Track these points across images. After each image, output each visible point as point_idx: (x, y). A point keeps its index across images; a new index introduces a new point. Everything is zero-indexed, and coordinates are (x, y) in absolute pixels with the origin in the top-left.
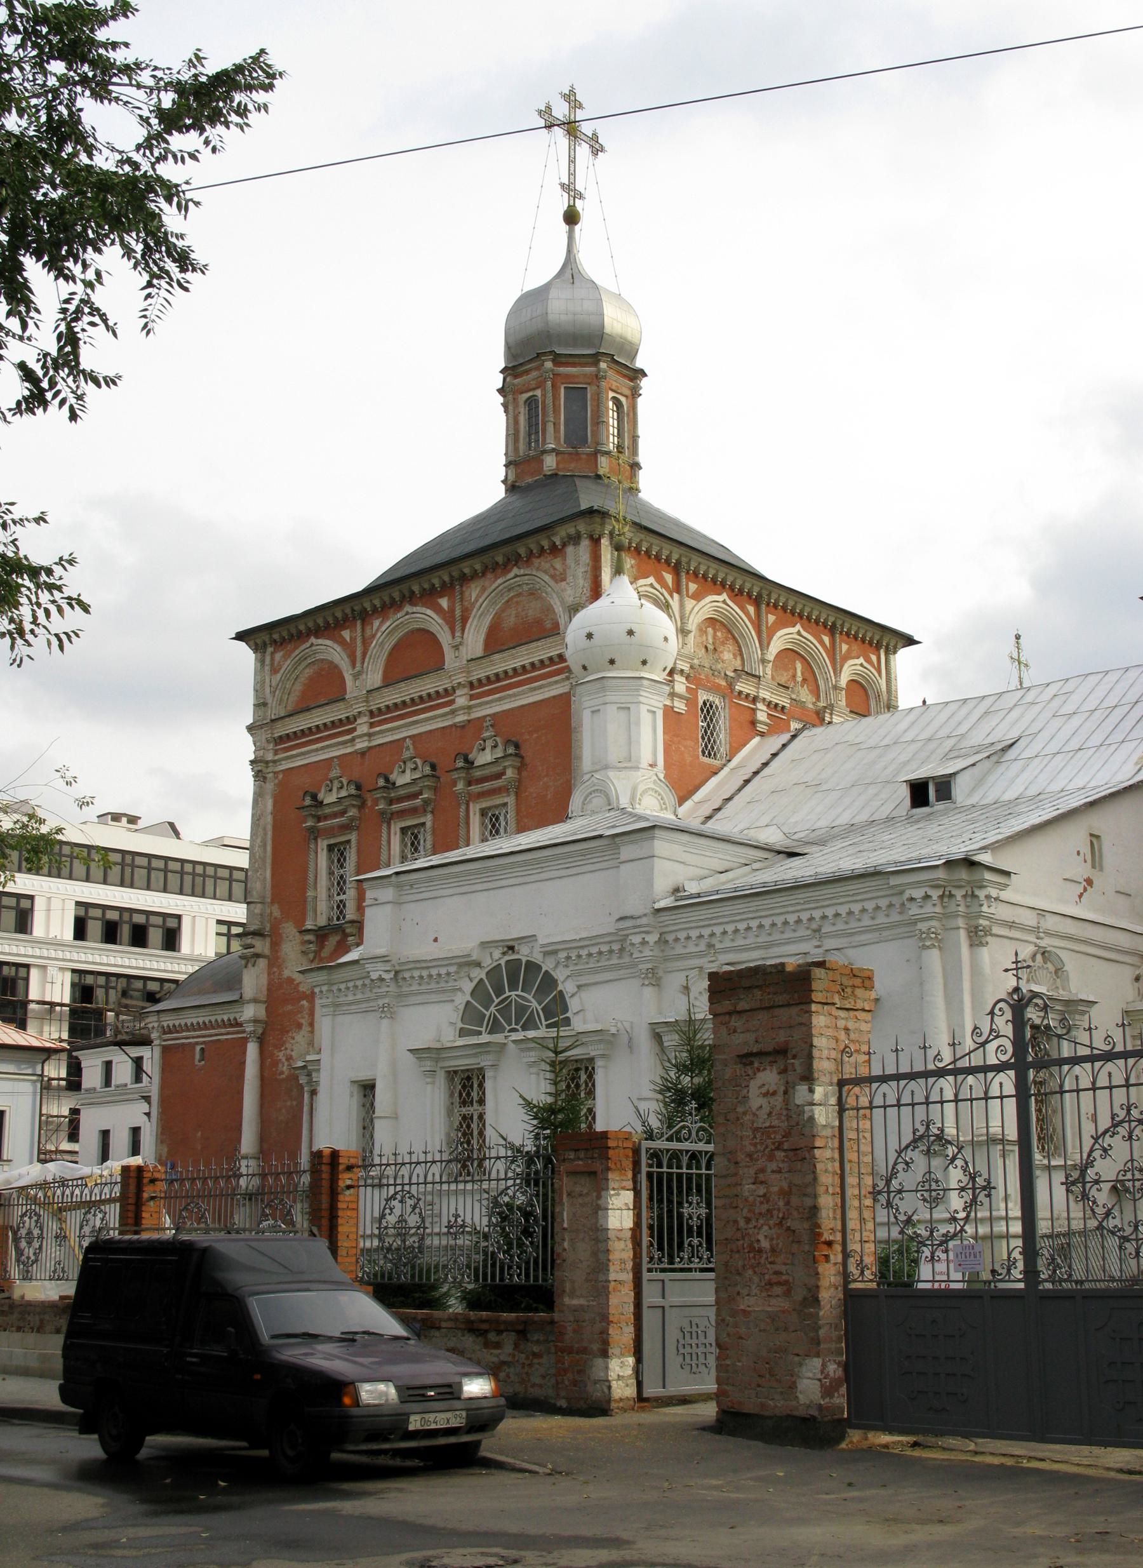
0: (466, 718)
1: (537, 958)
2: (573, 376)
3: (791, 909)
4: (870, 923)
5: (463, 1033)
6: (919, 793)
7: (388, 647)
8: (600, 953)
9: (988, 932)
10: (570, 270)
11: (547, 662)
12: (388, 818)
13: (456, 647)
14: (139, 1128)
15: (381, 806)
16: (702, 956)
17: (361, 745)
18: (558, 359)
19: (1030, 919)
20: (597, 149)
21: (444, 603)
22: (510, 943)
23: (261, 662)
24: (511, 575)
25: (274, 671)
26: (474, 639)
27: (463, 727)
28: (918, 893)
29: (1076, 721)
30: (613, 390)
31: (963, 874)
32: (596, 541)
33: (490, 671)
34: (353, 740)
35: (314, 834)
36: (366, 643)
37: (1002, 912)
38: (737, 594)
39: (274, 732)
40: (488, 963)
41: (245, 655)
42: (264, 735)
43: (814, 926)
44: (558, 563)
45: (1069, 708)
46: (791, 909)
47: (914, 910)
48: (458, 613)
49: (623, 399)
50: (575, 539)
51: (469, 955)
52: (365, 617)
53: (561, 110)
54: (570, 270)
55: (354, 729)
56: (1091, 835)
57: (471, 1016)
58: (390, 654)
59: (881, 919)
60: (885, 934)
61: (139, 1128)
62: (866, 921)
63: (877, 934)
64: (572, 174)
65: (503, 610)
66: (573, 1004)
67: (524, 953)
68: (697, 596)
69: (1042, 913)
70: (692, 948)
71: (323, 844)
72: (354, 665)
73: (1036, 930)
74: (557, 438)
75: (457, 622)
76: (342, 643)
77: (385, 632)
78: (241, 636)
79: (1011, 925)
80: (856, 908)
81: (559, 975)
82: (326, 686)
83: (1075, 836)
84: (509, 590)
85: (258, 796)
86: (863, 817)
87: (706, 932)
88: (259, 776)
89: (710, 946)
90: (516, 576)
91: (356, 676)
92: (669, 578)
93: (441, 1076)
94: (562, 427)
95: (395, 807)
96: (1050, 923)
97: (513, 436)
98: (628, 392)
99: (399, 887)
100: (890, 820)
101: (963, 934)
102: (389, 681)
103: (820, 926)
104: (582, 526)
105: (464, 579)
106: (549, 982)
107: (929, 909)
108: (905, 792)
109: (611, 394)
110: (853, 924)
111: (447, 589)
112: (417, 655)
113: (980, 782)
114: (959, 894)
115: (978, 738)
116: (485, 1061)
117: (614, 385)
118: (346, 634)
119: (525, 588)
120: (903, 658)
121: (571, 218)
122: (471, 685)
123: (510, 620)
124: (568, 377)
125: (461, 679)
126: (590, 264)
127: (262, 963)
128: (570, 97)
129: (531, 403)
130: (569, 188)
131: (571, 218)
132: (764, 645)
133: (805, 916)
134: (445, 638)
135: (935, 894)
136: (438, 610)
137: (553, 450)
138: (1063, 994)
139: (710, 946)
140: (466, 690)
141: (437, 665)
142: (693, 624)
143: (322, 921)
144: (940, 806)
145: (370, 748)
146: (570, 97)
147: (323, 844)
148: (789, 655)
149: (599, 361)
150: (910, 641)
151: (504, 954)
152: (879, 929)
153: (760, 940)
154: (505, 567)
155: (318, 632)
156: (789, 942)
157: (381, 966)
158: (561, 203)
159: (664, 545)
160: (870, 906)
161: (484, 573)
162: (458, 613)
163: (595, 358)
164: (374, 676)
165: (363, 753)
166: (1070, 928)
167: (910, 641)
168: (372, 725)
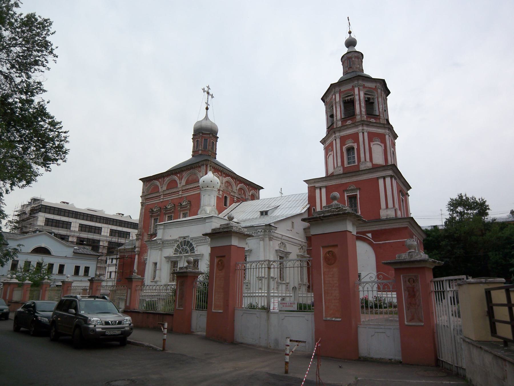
1: (189, 240)
5: (174, 254)
6: (262, 213)
9: (272, 238)
10: (206, 117)
12: (165, 214)
13: (180, 183)
14: (89, 268)
18: (203, 134)
19: (280, 236)
20: (212, 97)
21: (178, 175)
23: (144, 184)
25: (146, 186)
26: (183, 182)
28: (260, 230)
29: (290, 202)
31: (268, 227)
32: (207, 166)
33: (186, 188)
35: (152, 216)
36: (164, 182)
37: (276, 235)
38: (232, 178)
39: (145, 197)
40: (180, 241)
41: (141, 183)
42: (143, 198)
45: (289, 200)
47: (259, 233)
50: (203, 165)
52: (164, 177)
53: (206, 89)
54: (206, 117)
57: (176, 250)
61: (89, 268)
64: (208, 101)
66: (195, 249)
67: (187, 239)
68: (225, 177)
69: (283, 235)
71: (153, 219)
73: (281, 239)
75: (181, 179)
76: (159, 181)
78: (140, 179)
79: (277, 237)
81: (193, 243)
82: (156, 189)
83: (289, 223)
85: (142, 209)
86: (252, 217)
88: (142, 205)
91: (161, 188)
92: (220, 173)
93: (170, 262)
96: (284, 237)
97: (194, 147)
99: (164, 226)
100: (256, 218)
101: (268, 238)
102: (167, 189)
104: (204, 163)
105: (183, 171)
106: (191, 245)
107: (262, 233)
108: (259, 213)
111: (179, 173)
112: (173, 184)
113: (273, 212)
114: (267, 231)
115: (273, 205)
116: (178, 260)
118: (160, 180)
120: (261, 191)
121: (207, 109)
123: (190, 179)
125: (181, 189)
126: (210, 117)
127: (140, 240)
128: (208, 87)
129: (197, 141)
130: (207, 103)
131: (207, 109)
132: (237, 187)
134: (178, 181)
135: (263, 231)
136: (177, 176)
138: (286, 251)
141: (177, 187)
142: (224, 182)
143: (152, 233)
144: (266, 216)
146: (208, 87)
147: (153, 219)
148: (241, 189)
150: (263, 188)
154: (190, 169)
155: (155, 179)
163: (209, 134)
164: (165, 188)
165: (162, 202)
166: (288, 239)
167: (263, 188)
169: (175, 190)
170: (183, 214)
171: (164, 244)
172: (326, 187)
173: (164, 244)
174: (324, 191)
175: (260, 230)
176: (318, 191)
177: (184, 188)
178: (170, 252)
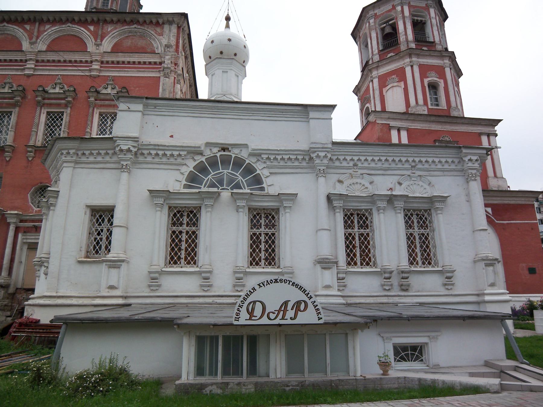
0: (98, 74)
3: (405, 155)
4: (441, 167)
5: (186, 186)
7: (53, 37)
8: (289, 159)
11: (147, 63)
12: (43, 105)
15: (39, 99)
16: (350, 169)
17: (27, 72)
22: (225, 146)
24: (133, 26)
26: (107, 45)
27: (95, 77)
34: (24, 69)
40: (208, 153)
43: (413, 164)
44: (158, 30)
46: (405, 155)
48: (100, 32)
51: (199, 147)
55: (26, 65)
58: (53, 40)
59: (446, 166)
60: (446, 173)
62: (439, 166)
63: (442, 173)
65: (124, 39)
67: (234, 153)
70: (345, 164)
72: (31, 39)
75: (99, 37)
77: (51, 31)
80: (437, 160)
84: (130, 32)
87: (356, 158)
89: (355, 165)
90: (135, 28)
95: (46, 101)
102: (50, 49)
103: (416, 165)
110: (433, 166)
119: (138, 34)
122: (102, 62)
123: (128, 43)
125: (98, 58)
133: (411, 159)
139: (355, 165)
140: (99, 63)
145: (33, 75)
151: (219, 151)
152: (443, 171)
153: (384, 166)
156: (399, 169)
157: (131, 143)
160: (443, 160)
161: (117, 23)
162: (100, 32)
164: (42, 46)
165: (28, 76)
168: (36, 66)
169: (77, 57)
170: (101, 114)
171: (141, 154)
173: (141, 154)
175: (474, 158)
177: (105, 59)
178: (172, 179)
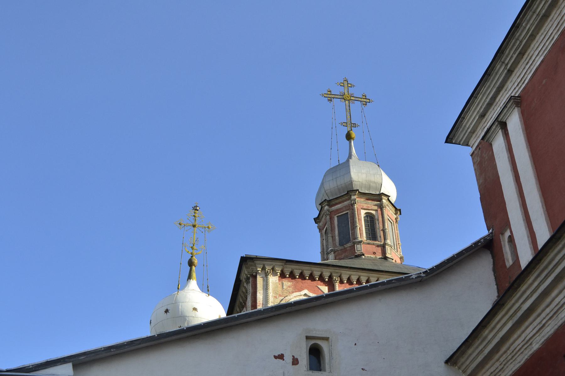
2: (340, 209)
18: (330, 203)
30: (364, 209)
32: (255, 277)
49: (373, 212)
53: (337, 90)
56: (308, 338)
74: (334, 245)
94: (337, 238)
98: (376, 208)
109: (363, 212)
117: (365, 206)
121: (349, 137)
124: (337, 211)
131: (349, 137)
137: (332, 251)
146: (346, 83)
149: (351, 196)
158: (345, 131)
159: (313, 269)
172: (516, 101)
174: (515, 122)
176: (498, 144)
